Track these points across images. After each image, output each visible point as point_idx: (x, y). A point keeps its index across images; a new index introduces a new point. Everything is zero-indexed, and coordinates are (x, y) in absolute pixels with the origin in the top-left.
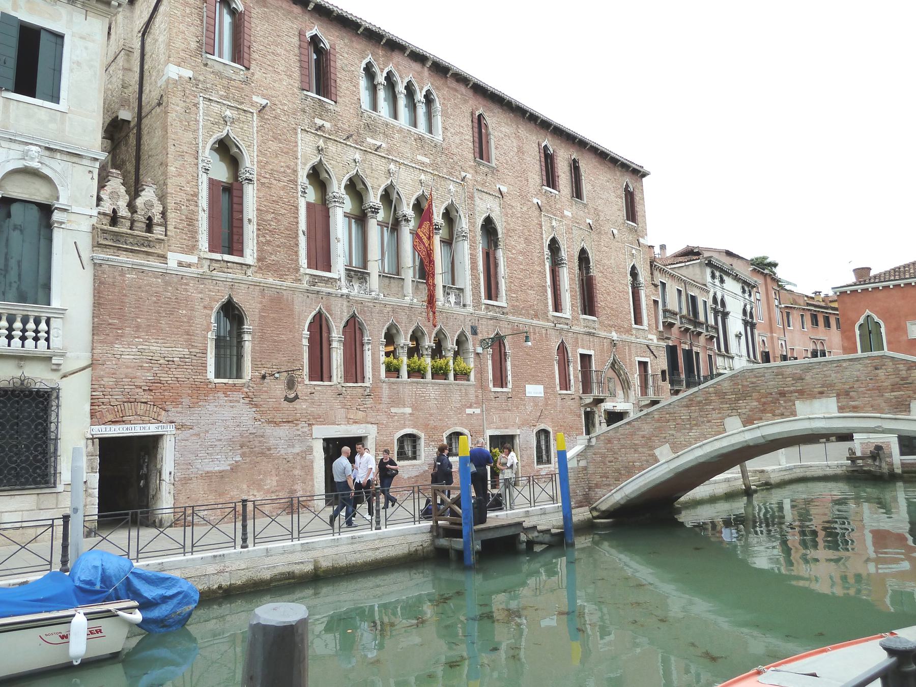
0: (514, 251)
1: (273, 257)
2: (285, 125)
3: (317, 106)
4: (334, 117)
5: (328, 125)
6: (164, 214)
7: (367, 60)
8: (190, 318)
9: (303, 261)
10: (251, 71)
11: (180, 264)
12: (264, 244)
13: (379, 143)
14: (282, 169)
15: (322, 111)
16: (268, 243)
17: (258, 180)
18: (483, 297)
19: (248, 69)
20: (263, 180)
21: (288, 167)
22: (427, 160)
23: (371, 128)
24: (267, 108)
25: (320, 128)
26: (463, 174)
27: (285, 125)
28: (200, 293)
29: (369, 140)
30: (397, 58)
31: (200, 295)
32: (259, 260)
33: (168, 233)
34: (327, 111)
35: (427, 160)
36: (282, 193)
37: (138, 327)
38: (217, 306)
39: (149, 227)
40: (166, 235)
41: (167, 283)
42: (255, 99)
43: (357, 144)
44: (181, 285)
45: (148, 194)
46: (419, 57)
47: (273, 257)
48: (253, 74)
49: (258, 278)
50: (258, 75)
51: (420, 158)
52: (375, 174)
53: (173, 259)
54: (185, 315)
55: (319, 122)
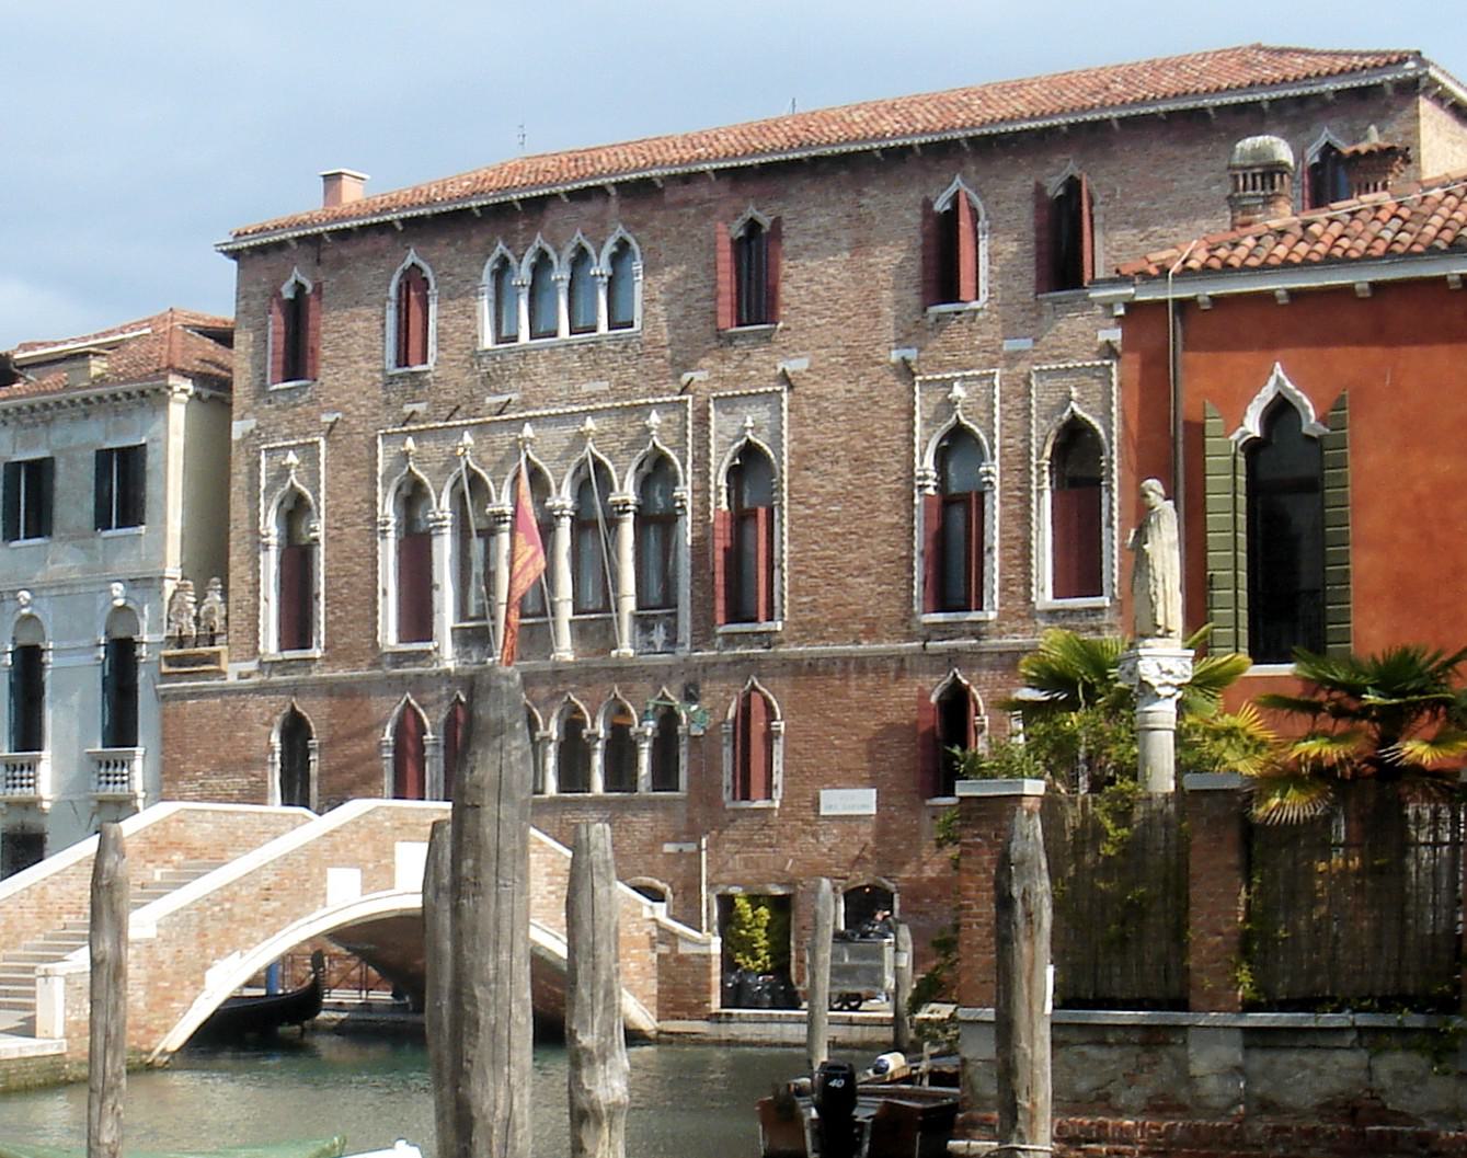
0: (813, 500)
2: (362, 437)
5: (421, 408)
6: (226, 618)
7: (497, 253)
8: (248, 740)
13: (505, 398)
14: (357, 507)
16: (339, 620)
18: (720, 618)
22: (605, 386)
29: (490, 400)
30: (553, 216)
35: (605, 386)
36: (357, 542)
43: (468, 417)
47: (345, 640)
51: (586, 388)
55: (408, 409)
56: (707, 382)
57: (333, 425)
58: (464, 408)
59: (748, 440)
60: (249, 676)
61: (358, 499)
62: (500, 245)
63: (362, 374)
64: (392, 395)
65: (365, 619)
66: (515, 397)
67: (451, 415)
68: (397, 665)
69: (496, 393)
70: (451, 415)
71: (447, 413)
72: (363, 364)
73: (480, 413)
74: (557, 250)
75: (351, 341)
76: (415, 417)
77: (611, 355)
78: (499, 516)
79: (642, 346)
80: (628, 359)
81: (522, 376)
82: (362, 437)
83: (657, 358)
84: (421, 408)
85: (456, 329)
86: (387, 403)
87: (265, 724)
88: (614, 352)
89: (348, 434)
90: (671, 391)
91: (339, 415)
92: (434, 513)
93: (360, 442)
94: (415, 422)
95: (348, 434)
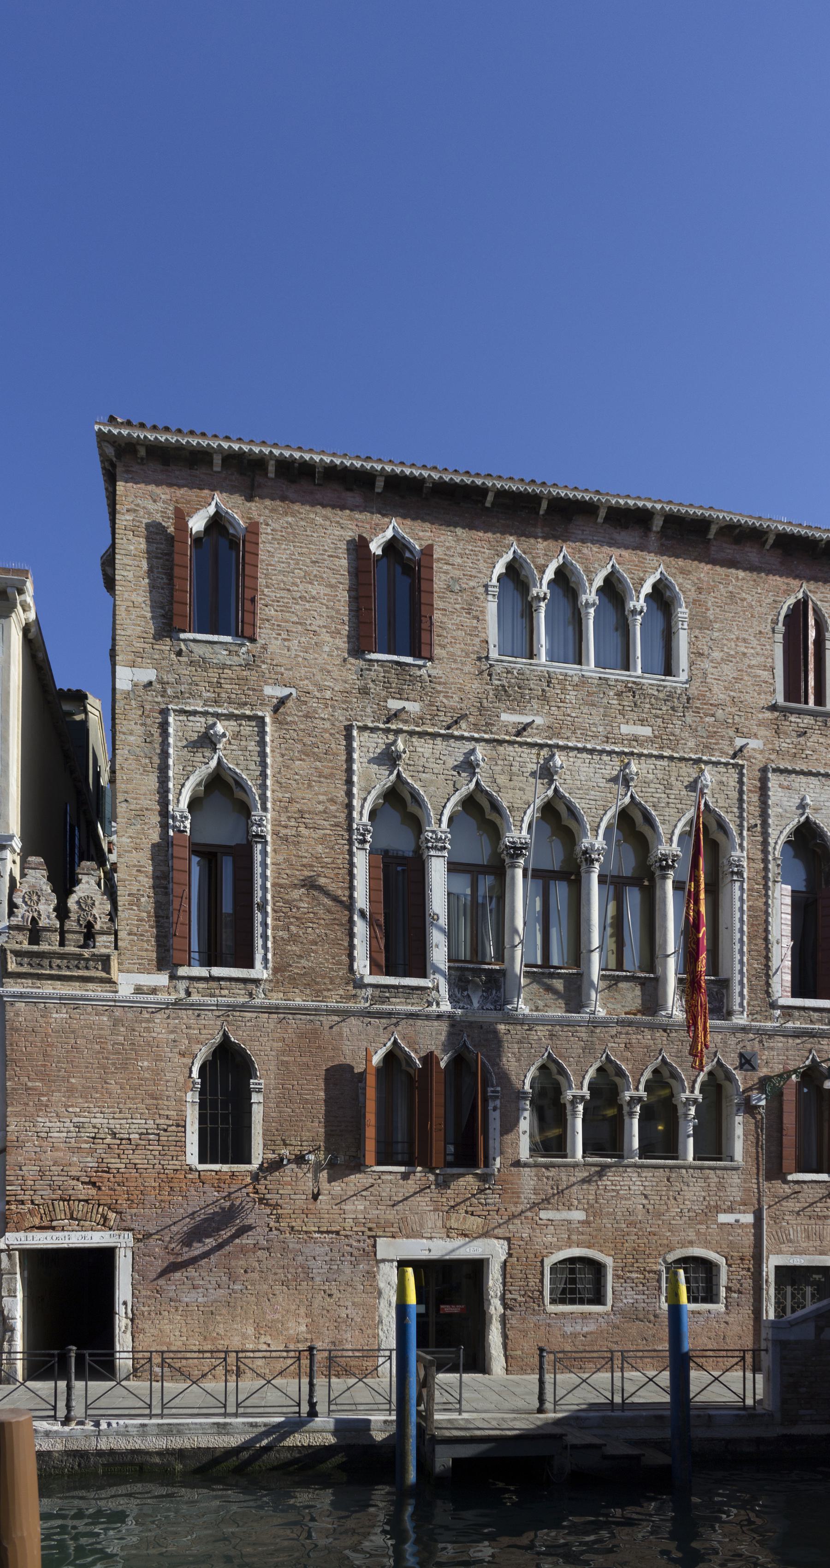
1: (304, 962)
3: (392, 676)
4: (426, 689)
5: (413, 707)
9: (362, 965)
10: (261, 641)
11: (139, 990)
12: (286, 942)
14: (321, 808)
15: (403, 681)
17: (275, 833)
19: (253, 640)
20: (284, 831)
21: (332, 801)
22: (646, 731)
23: (512, 693)
24: (290, 703)
25: (395, 715)
26: (739, 742)
27: (328, 725)
28: (172, 1032)
29: (505, 717)
31: (172, 1036)
32: (276, 970)
33: (120, 943)
34: (414, 679)
35: (646, 731)
36: (320, 849)
37: (71, 1090)
38: (203, 1053)
39: (89, 934)
40: (116, 948)
41: (116, 1022)
42: (268, 690)
43: (479, 731)
44: (141, 1022)
45: (88, 886)
46: (629, 523)
48: (264, 647)
49: (276, 999)
50: (275, 646)
51: (625, 729)
52: (518, 782)
53: (126, 983)
54: (148, 1068)
55: (394, 704)
56: (762, 752)
57: (282, 701)
58: (471, 719)
59: (807, 818)
60: (154, 991)
61: (322, 798)
62: (515, 546)
63: (326, 649)
64: (371, 685)
65: (335, 942)
66: (539, 721)
67: (456, 722)
68: (384, 1000)
69: (513, 710)
70: (456, 722)
71: (450, 721)
72: (327, 638)
73: (494, 729)
74: (588, 571)
75: (307, 605)
76: (404, 716)
77: (653, 701)
78: (521, 848)
79: (688, 699)
80: (673, 708)
81: (544, 697)
82: (328, 725)
83: (706, 715)
84: (413, 707)
85: (460, 626)
86: (364, 691)
87: (182, 1055)
88: (657, 698)
89: (306, 716)
90: (723, 753)
91: (293, 691)
92: (433, 832)
93: (325, 730)
94: (406, 722)
95: (306, 716)
